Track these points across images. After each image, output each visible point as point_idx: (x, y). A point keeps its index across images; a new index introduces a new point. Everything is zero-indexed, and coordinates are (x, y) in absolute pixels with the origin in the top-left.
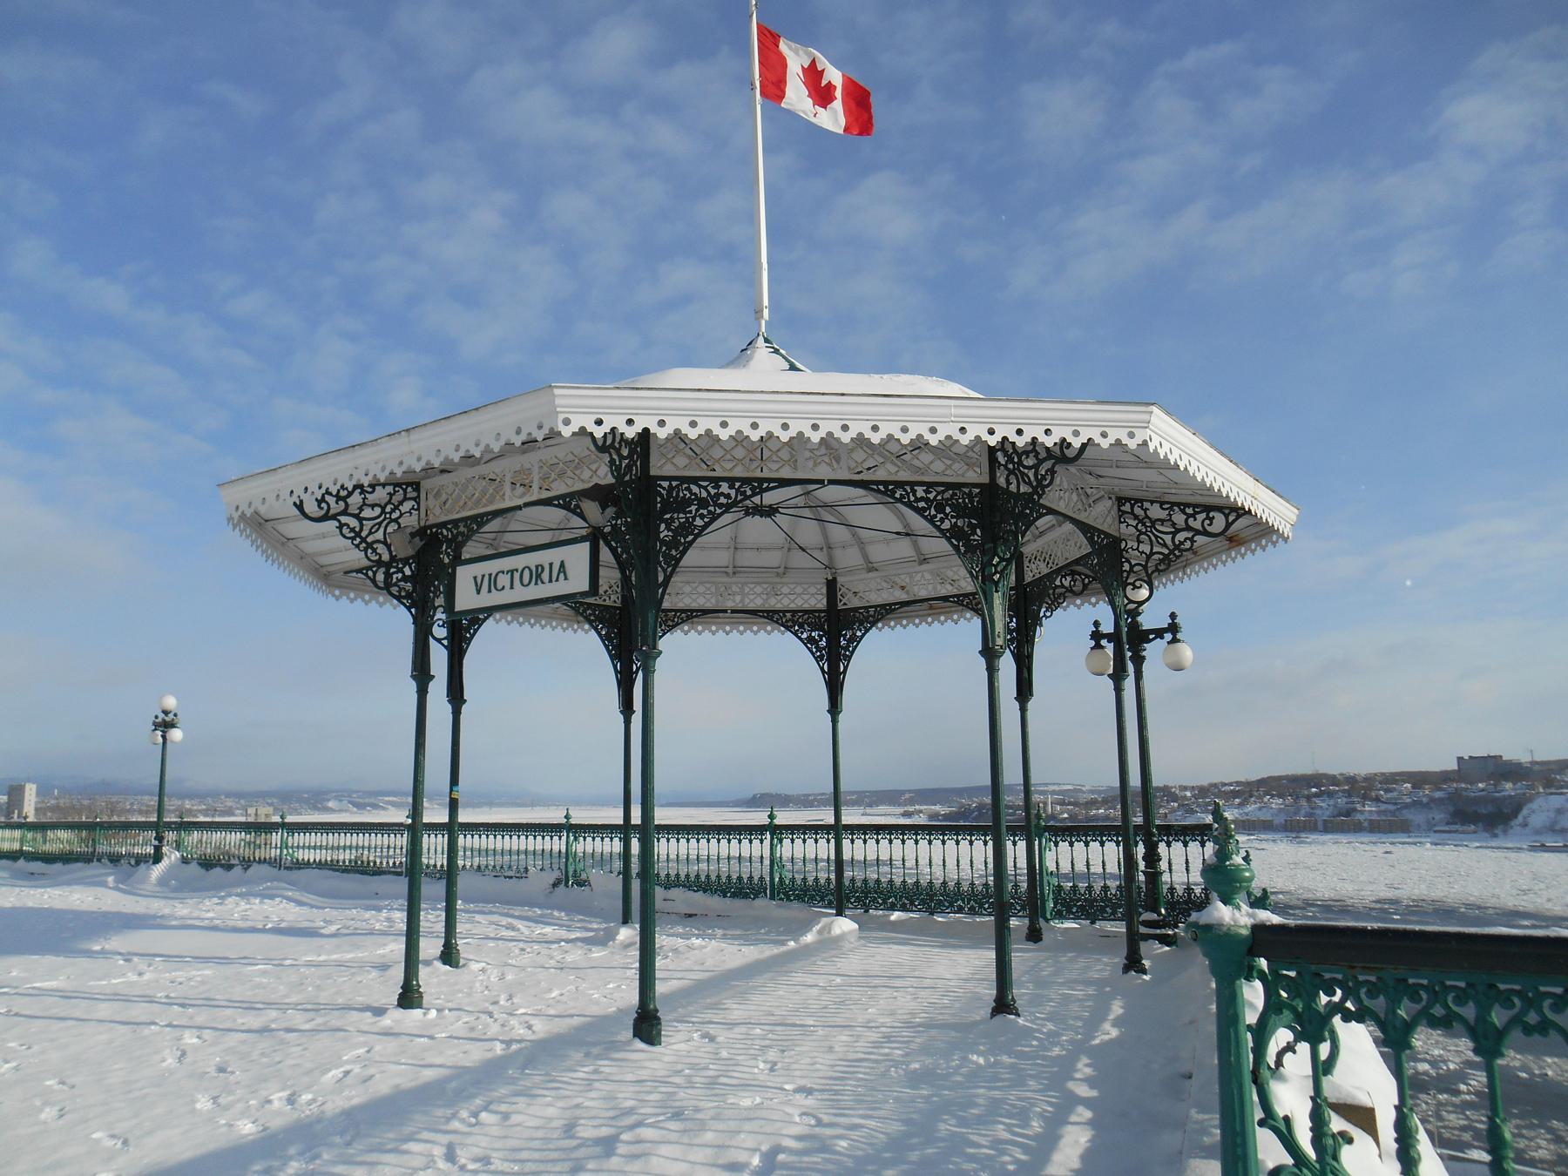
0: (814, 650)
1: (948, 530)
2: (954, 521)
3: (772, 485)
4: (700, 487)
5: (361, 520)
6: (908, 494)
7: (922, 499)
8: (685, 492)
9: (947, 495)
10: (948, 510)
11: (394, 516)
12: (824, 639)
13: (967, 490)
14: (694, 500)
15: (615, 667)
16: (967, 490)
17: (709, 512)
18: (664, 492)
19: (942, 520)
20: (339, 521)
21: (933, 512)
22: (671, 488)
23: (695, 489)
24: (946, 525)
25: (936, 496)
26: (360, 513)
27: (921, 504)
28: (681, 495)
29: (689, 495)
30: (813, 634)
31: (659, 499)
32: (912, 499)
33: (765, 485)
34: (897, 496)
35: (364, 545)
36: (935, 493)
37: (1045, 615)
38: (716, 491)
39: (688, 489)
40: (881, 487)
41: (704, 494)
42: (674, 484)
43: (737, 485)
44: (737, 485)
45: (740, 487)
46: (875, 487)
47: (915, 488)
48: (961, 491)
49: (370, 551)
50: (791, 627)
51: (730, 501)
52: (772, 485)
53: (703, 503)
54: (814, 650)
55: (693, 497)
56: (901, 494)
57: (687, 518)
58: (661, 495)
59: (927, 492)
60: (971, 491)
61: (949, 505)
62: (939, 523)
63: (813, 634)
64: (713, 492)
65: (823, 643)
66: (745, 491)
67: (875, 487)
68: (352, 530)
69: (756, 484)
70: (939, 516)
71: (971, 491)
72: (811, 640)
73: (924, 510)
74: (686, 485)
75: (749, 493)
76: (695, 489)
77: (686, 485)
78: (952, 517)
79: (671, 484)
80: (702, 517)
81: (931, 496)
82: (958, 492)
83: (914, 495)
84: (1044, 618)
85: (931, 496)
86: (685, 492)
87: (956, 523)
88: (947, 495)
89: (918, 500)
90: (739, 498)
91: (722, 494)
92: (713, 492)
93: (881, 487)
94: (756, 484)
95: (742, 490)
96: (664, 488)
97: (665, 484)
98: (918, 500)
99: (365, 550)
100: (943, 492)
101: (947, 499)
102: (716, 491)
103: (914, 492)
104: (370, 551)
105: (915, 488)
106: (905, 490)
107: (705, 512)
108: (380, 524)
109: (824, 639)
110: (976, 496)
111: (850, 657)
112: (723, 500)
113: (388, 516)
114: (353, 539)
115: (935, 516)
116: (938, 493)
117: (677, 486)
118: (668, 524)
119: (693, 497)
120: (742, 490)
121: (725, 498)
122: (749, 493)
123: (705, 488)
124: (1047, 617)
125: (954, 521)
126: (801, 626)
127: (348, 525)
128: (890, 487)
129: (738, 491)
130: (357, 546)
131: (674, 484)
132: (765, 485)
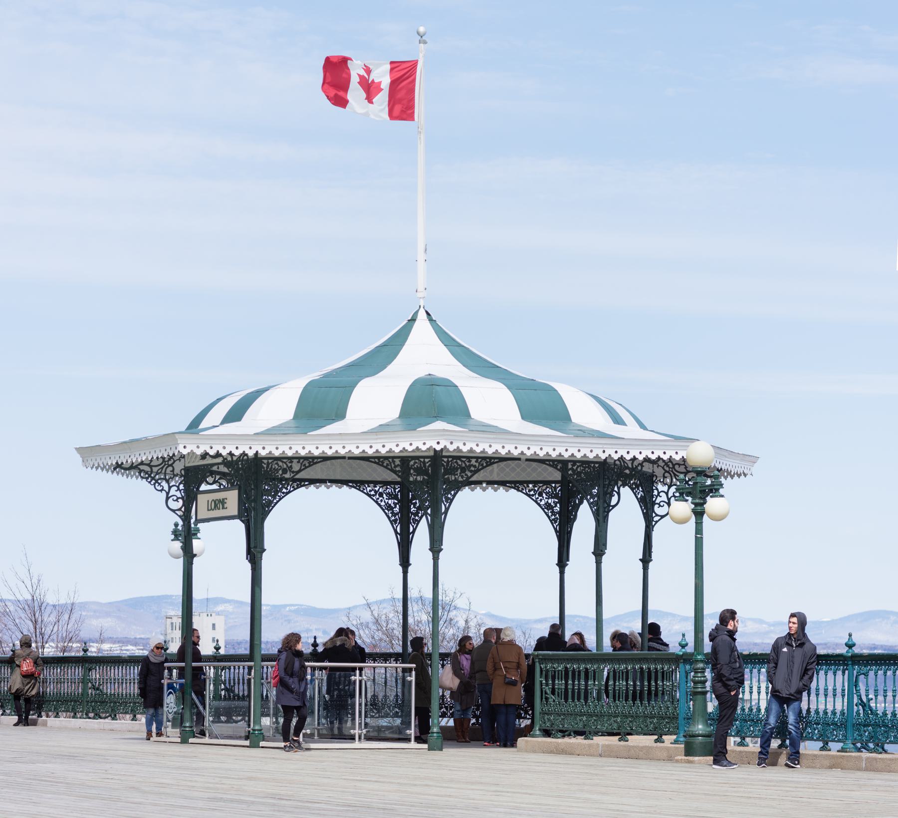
0: (550, 514)
2: (415, 477)
4: (283, 462)
5: (151, 467)
6: (391, 463)
11: (170, 463)
12: (558, 505)
13: (422, 460)
15: (395, 531)
16: (422, 460)
18: (265, 466)
20: (139, 469)
23: (280, 463)
26: (150, 463)
28: (273, 467)
30: (550, 501)
32: (393, 466)
34: (385, 464)
35: (153, 481)
39: (277, 464)
40: (377, 460)
41: (285, 466)
47: (395, 460)
49: (157, 484)
50: (533, 495)
54: (550, 514)
60: (424, 460)
63: (550, 501)
65: (557, 509)
66: (305, 464)
67: (373, 460)
68: (146, 473)
71: (424, 460)
72: (548, 506)
74: (276, 462)
77: (276, 462)
78: (414, 475)
82: (417, 461)
83: (394, 464)
87: (416, 479)
89: (395, 467)
92: (289, 465)
93: (377, 460)
98: (395, 467)
99: (154, 484)
103: (394, 462)
104: (157, 484)
105: (395, 460)
106: (389, 461)
108: (162, 468)
109: (558, 505)
110: (428, 462)
113: (167, 463)
114: (147, 478)
117: (271, 463)
122: (307, 465)
123: (285, 463)
126: (540, 494)
127: (143, 470)
128: (381, 460)
130: (150, 482)
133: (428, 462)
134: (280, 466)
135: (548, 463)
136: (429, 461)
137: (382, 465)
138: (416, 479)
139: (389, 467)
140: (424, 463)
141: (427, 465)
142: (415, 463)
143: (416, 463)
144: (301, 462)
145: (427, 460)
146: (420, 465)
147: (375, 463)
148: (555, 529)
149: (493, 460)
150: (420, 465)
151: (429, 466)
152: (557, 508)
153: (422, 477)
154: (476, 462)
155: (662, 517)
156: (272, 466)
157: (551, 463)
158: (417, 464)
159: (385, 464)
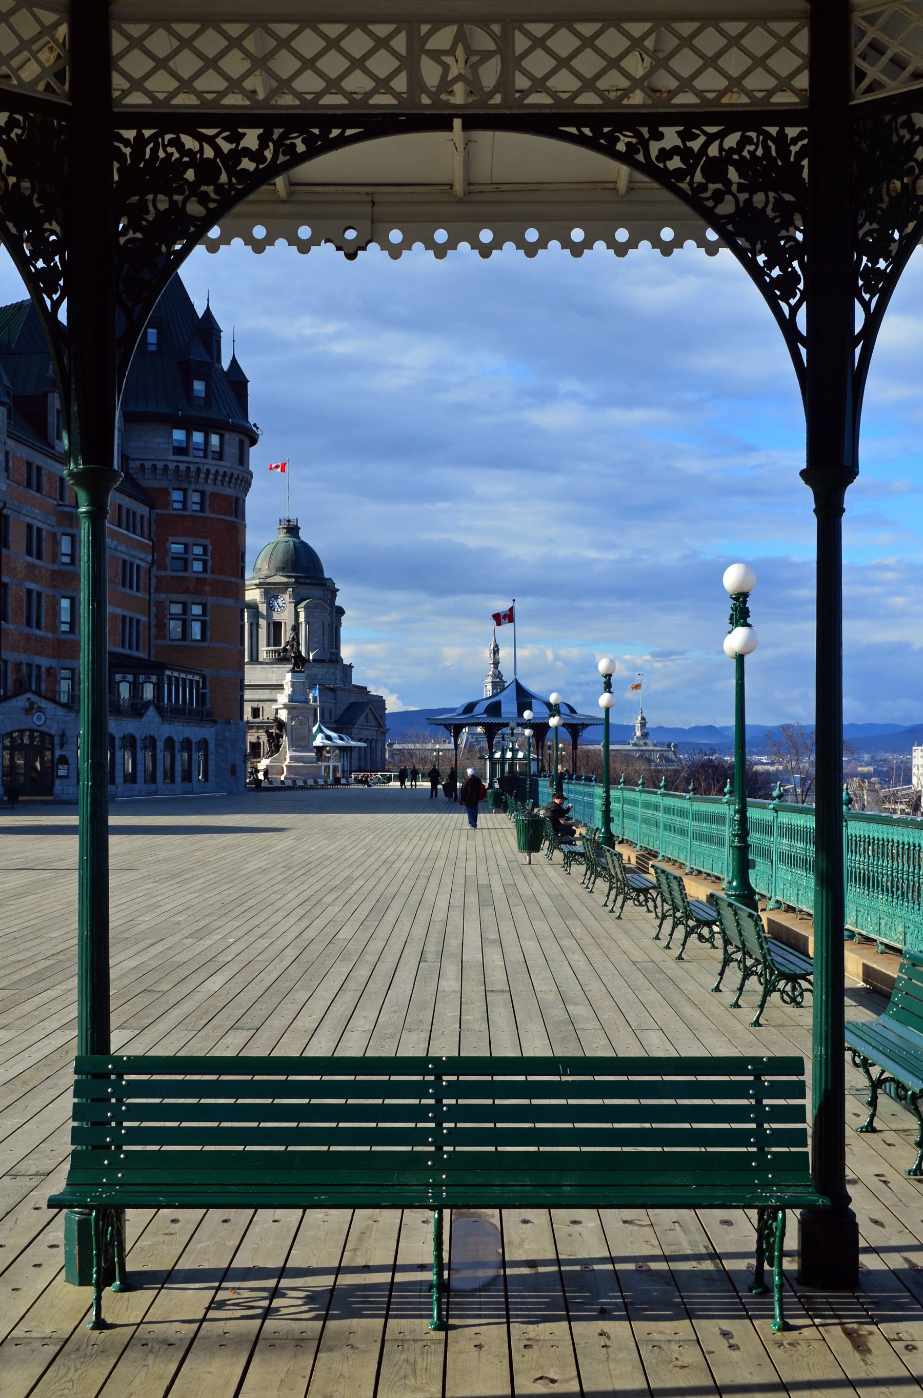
1: (729, 217)
2: (743, 197)
3: (349, 132)
4: (201, 138)
7: (675, 150)
8: (170, 150)
9: (732, 140)
10: (733, 174)
13: (773, 130)
14: (187, 166)
16: (773, 130)
17: (219, 189)
19: (718, 197)
21: (698, 177)
22: (140, 142)
23: (189, 142)
24: (727, 207)
25: (705, 146)
27: (675, 163)
28: (162, 154)
29: (176, 155)
31: (116, 165)
33: (335, 132)
34: (621, 147)
36: (702, 139)
38: (233, 146)
41: (209, 153)
42: (147, 133)
43: (277, 132)
44: (277, 132)
45: (283, 136)
46: (573, 130)
48: (760, 132)
51: (261, 166)
52: (349, 132)
53: (207, 170)
55: (186, 159)
56: (628, 144)
57: (173, 203)
58: (121, 157)
59: (686, 136)
61: (735, 164)
62: (710, 204)
64: (226, 147)
66: (294, 145)
67: (573, 130)
69: (316, 131)
70: (712, 187)
71: (781, 133)
73: (679, 174)
75: (301, 148)
76: (189, 142)
79: (140, 135)
80: (204, 199)
81: (696, 145)
82: (753, 135)
85: (696, 145)
86: (170, 150)
87: (749, 201)
88: (732, 140)
90: (282, 159)
91: (247, 152)
92: (226, 147)
93: (587, 131)
94: (316, 131)
95: (288, 142)
96: (126, 142)
97: (130, 134)
100: (721, 136)
102: (233, 146)
106: (638, 135)
107: (210, 189)
110: (795, 141)
112: (247, 164)
115: (703, 188)
116: (711, 138)
117: (153, 138)
118: (136, 215)
119: (186, 159)
120: (288, 142)
121: (251, 160)
122: (301, 148)
123: (211, 141)
125: (743, 197)
129: (278, 144)
131: (147, 133)
132: (335, 132)
133: (795, 141)
134: (190, 153)
136: (801, 136)
137: (610, 151)
138: (749, 201)
139: (640, 157)
140: (782, 141)
141: (794, 149)
143: (750, 141)
144: (275, 137)
145: (792, 132)
146: (767, 149)
147: (580, 140)
150: (767, 149)
151: (800, 155)
153: (772, 195)
156: (154, 151)
158: (752, 148)
159: (621, 147)
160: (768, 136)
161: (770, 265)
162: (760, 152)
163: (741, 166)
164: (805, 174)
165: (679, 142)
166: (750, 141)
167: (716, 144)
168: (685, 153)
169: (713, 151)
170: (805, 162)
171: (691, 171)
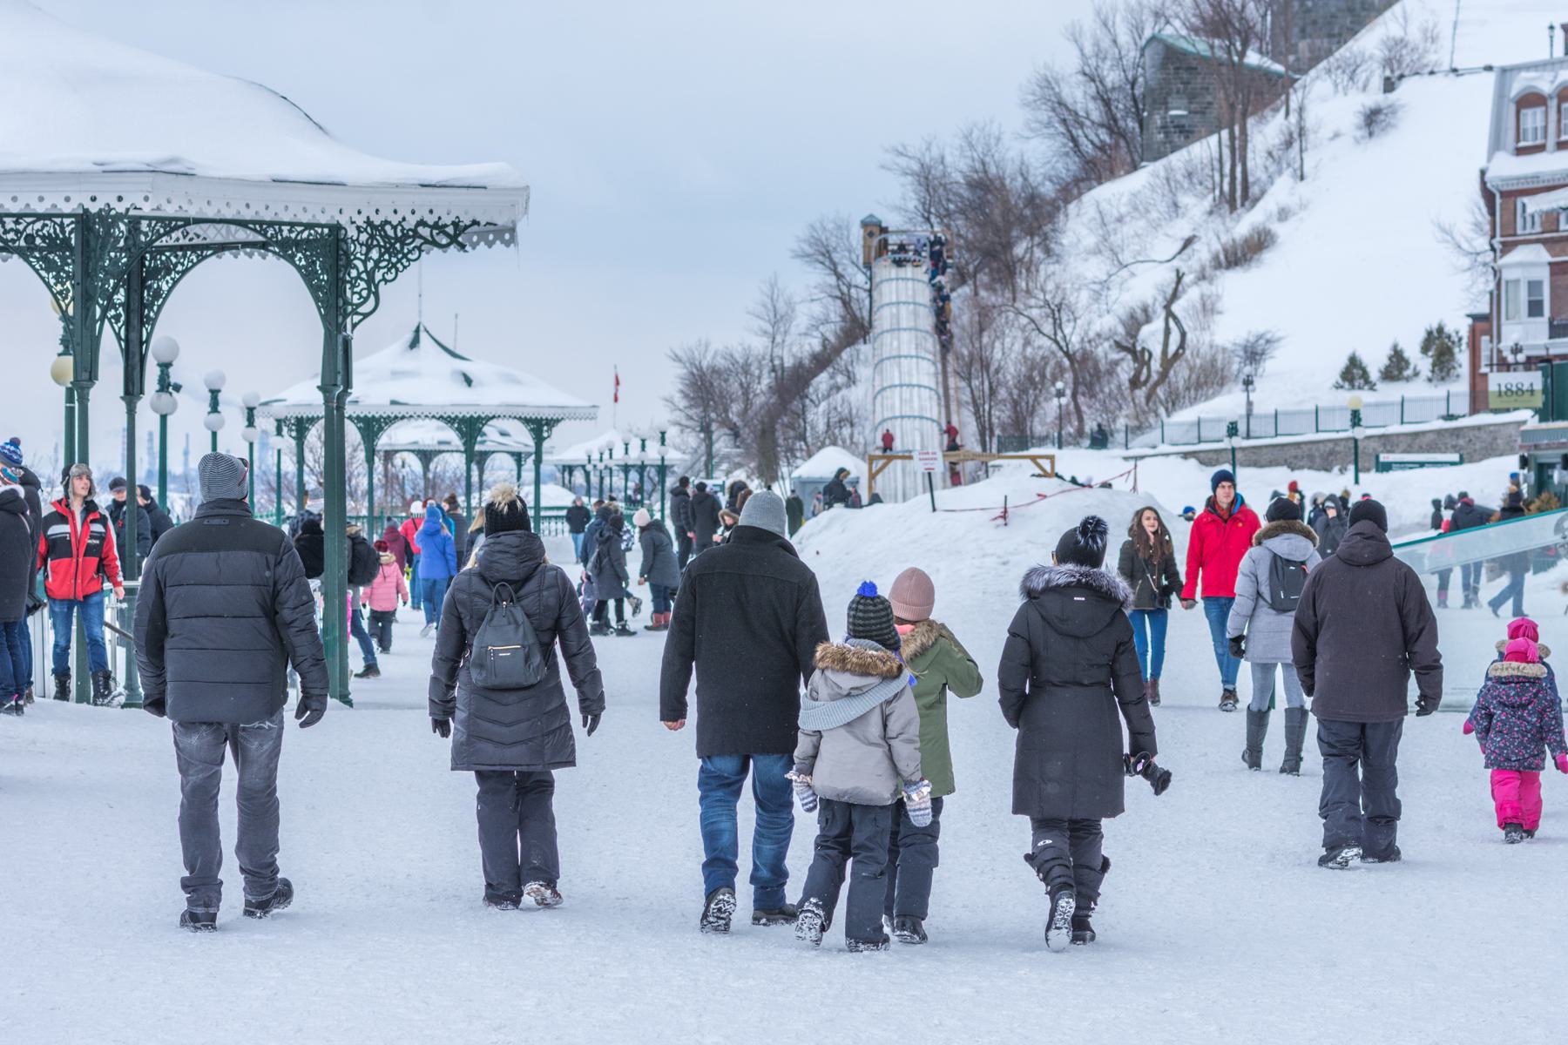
7: (12, 230)
9: (38, 225)
16: (58, 220)
25: (25, 229)
27: (11, 236)
36: (25, 224)
37: (384, 279)
59: (17, 223)
60: (62, 222)
71: (62, 222)
82: (48, 222)
84: (383, 283)
100: (33, 222)
101: (38, 231)
110: (68, 225)
111: (155, 320)
116: (29, 224)
124: (386, 281)
133: (68, 225)
135: (251, 226)
136: (72, 223)
140: (62, 225)
141: (68, 230)
142: (45, 225)
143: (47, 225)
145: (67, 221)
148: (118, 335)
149: (174, 223)
151: (70, 233)
152: (119, 296)
154: (149, 225)
155: (366, 316)
157: (257, 227)
160: (55, 223)
161: (56, 284)
162: (52, 231)
163: (43, 238)
164: (73, 242)
165: (13, 226)
166: (47, 225)
167: (30, 227)
168: (17, 232)
169: (29, 231)
170: (73, 236)
171: (19, 239)
